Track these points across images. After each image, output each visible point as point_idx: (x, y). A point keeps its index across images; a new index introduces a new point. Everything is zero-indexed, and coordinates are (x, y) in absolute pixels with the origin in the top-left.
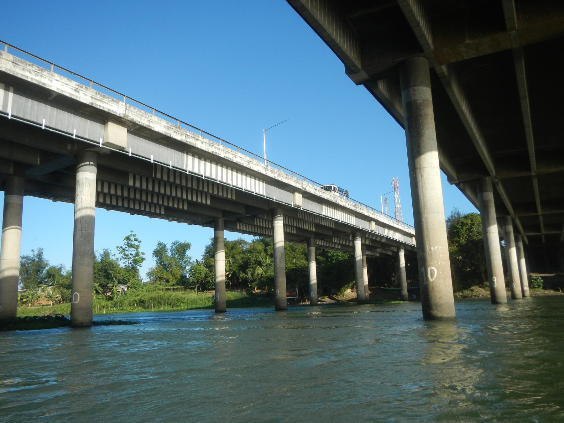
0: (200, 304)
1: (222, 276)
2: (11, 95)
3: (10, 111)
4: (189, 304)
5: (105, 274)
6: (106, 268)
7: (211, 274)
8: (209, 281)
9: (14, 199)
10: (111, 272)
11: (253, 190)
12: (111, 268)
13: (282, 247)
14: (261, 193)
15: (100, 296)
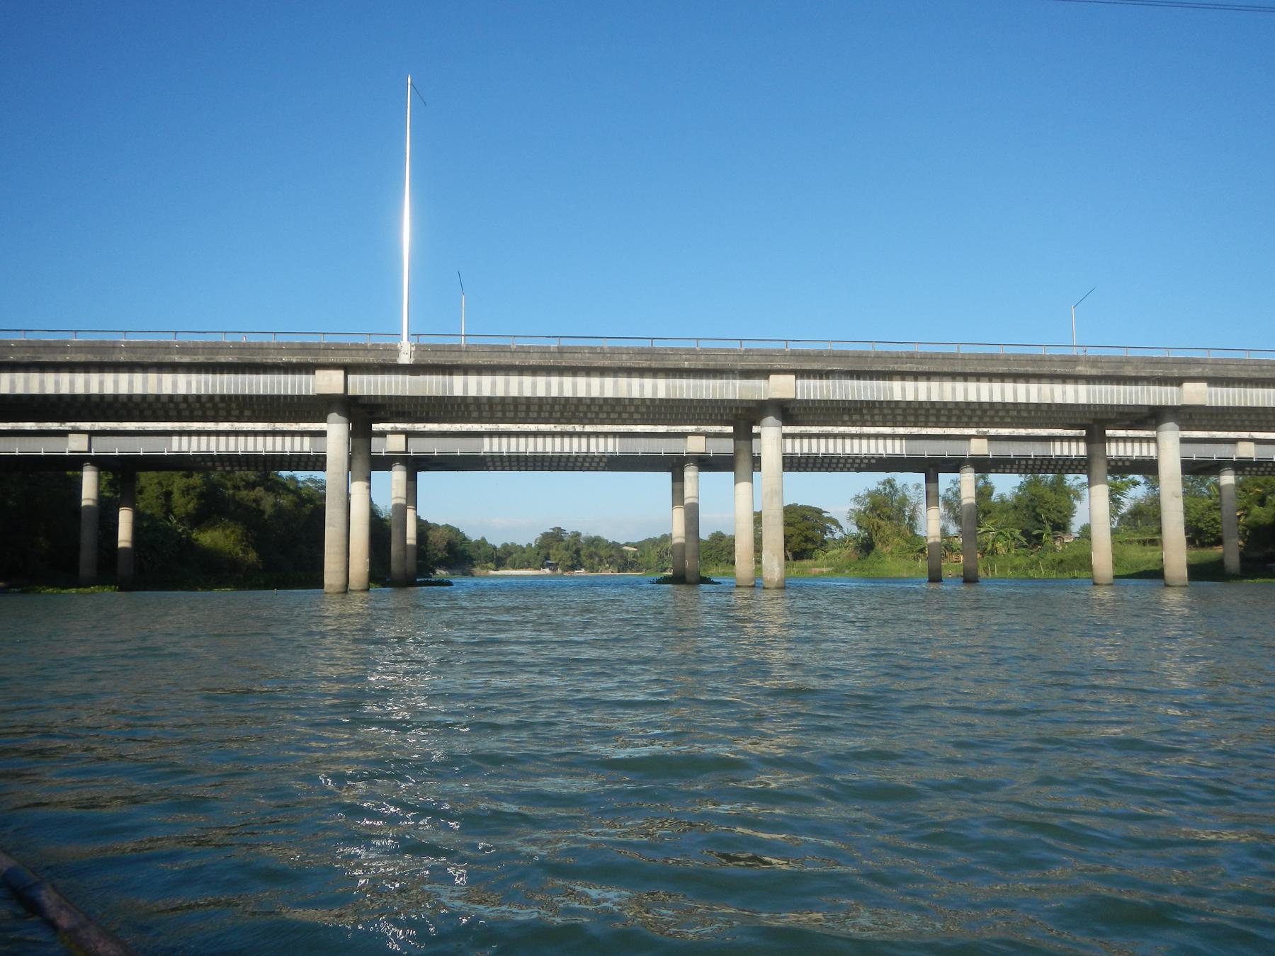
0: (1142, 568)
1: (934, 537)
2: (617, 440)
3: (617, 451)
4: (1127, 569)
5: (1033, 514)
6: (1033, 504)
7: (1207, 516)
8: (1202, 529)
9: (678, 485)
10: (1038, 510)
11: (881, 451)
12: (1041, 504)
13: (970, 505)
14: (898, 451)
15: (1021, 551)
